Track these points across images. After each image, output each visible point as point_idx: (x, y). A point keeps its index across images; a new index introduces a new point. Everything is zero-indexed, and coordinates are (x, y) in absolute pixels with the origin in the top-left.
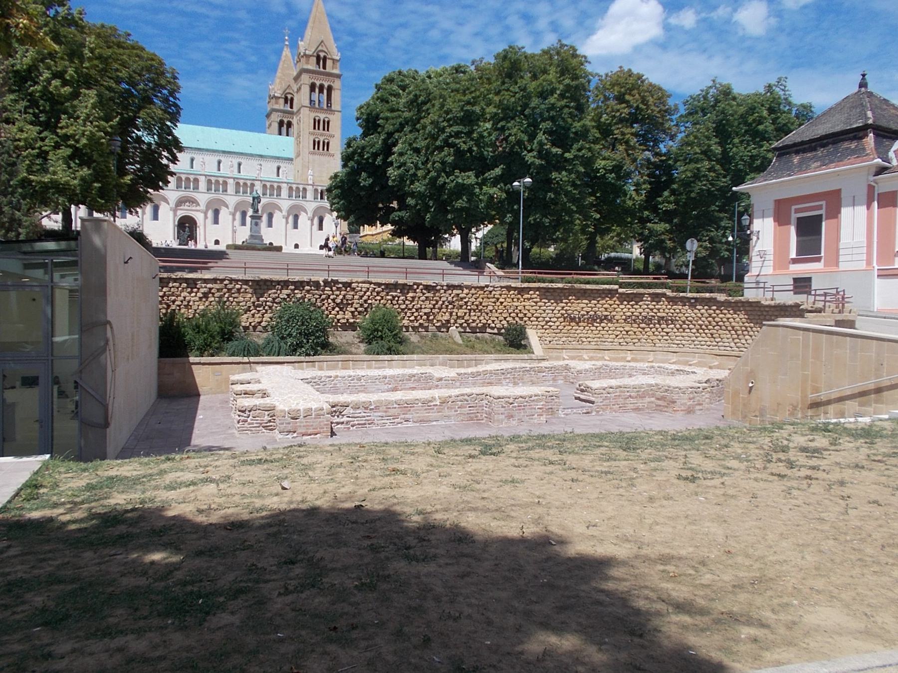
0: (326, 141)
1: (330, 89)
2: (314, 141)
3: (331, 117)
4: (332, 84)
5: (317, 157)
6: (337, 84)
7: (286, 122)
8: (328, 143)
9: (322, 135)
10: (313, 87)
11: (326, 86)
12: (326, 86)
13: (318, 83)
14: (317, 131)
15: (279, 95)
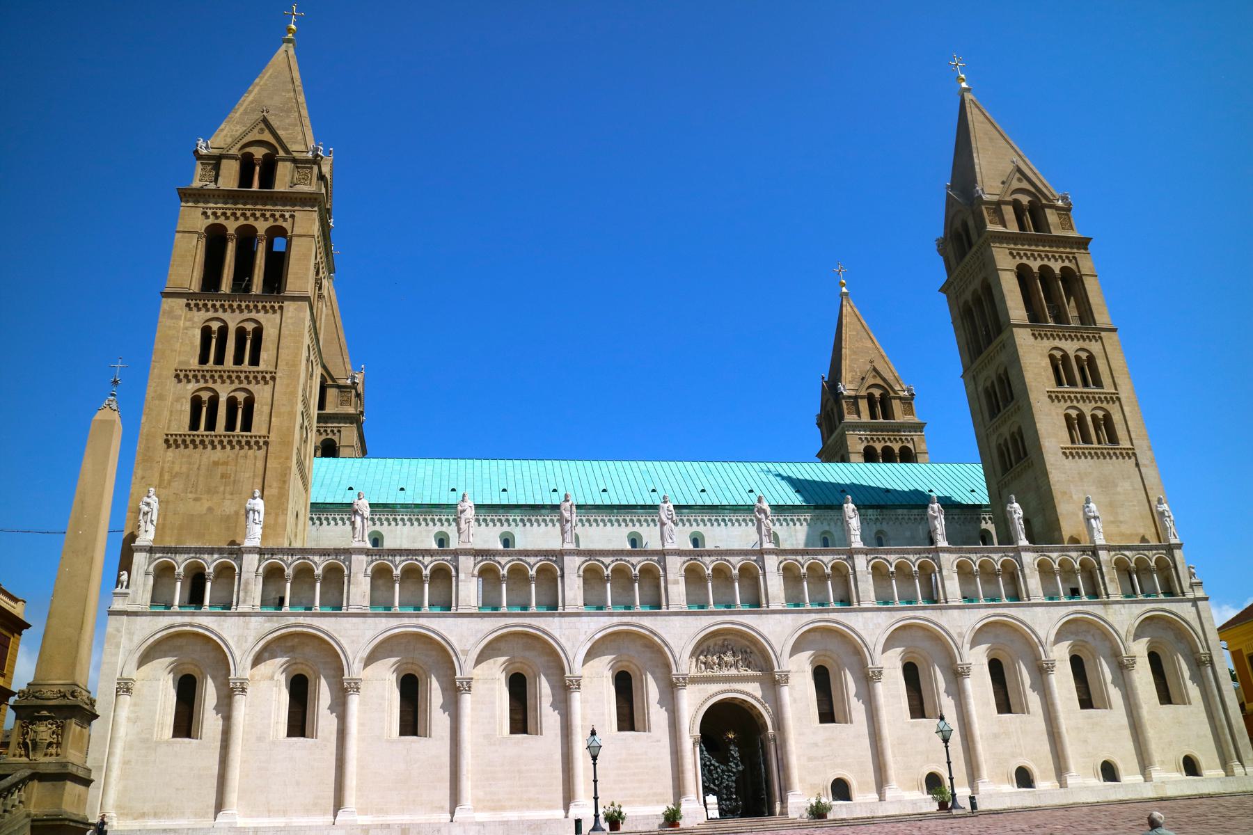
0: (1100, 414)
1: (1072, 280)
2: (1068, 418)
3: (1095, 347)
4: (1067, 263)
5: (1084, 464)
6: (1086, 264)
7: (879, 451)
8: (1108, 418)
9: (1085, 398)
10: (1023, 274)
11: (1057, 271)
12: (1057, 271)
13: (1035, 265)
14: (1066, 388)
15: (853, 393)
